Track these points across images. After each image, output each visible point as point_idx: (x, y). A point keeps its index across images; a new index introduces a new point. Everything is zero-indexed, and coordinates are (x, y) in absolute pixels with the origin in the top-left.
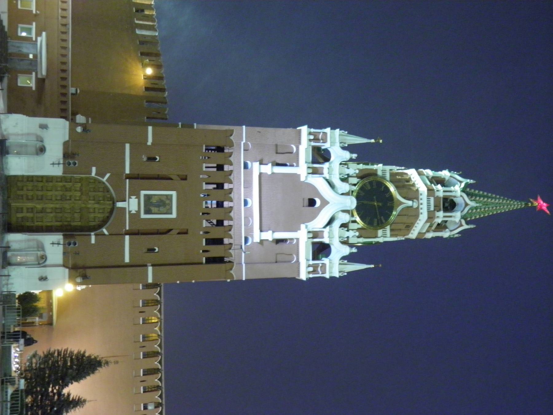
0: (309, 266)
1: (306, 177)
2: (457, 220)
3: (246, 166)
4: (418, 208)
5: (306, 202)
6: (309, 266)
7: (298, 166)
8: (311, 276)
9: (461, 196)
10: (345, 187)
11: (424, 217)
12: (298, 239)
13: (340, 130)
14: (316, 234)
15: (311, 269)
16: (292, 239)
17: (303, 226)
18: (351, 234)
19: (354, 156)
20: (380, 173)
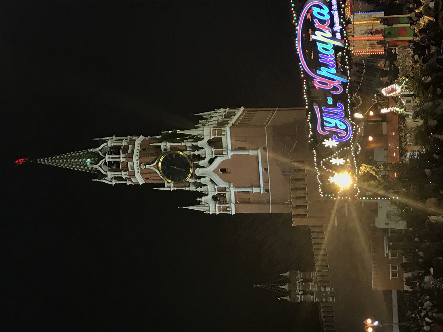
0: (224, 135)
1: (230, 186)
2: (107, 156)
3: (267, 190)
4: (140, 164)
5: (228, 171)
6: (224, 135)
7: (235, 192)
8: (223, 129)
9: (106, 172)
10: (202, 181)
11: (135, 159)
12: (232, 150)
13: (209, 214)
14: (222, 154)
15: (223, 133)
16: (236, 150)
17: (230, 158)
18: (196, 153)
19: (198, 199)
20: (172, 185)
